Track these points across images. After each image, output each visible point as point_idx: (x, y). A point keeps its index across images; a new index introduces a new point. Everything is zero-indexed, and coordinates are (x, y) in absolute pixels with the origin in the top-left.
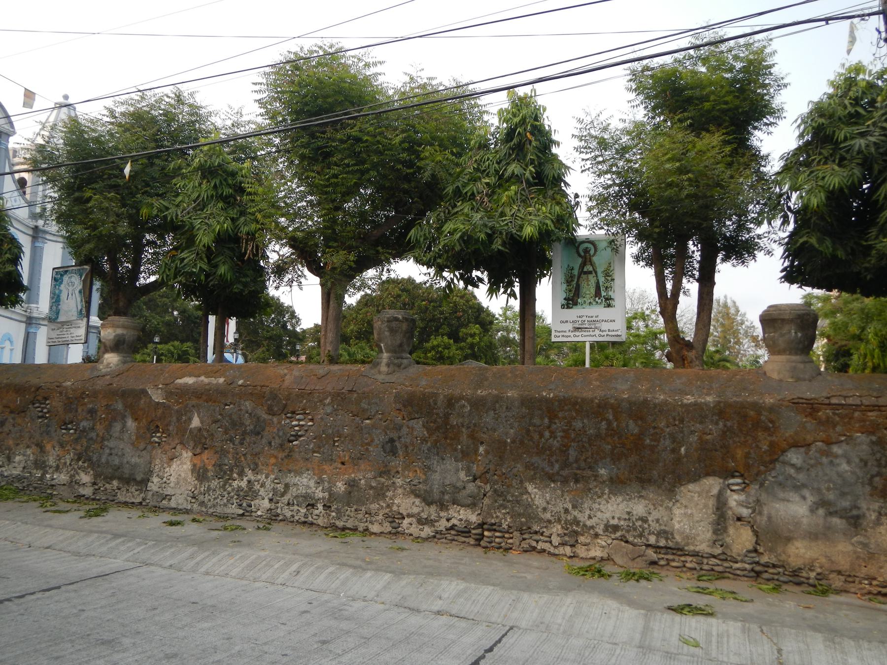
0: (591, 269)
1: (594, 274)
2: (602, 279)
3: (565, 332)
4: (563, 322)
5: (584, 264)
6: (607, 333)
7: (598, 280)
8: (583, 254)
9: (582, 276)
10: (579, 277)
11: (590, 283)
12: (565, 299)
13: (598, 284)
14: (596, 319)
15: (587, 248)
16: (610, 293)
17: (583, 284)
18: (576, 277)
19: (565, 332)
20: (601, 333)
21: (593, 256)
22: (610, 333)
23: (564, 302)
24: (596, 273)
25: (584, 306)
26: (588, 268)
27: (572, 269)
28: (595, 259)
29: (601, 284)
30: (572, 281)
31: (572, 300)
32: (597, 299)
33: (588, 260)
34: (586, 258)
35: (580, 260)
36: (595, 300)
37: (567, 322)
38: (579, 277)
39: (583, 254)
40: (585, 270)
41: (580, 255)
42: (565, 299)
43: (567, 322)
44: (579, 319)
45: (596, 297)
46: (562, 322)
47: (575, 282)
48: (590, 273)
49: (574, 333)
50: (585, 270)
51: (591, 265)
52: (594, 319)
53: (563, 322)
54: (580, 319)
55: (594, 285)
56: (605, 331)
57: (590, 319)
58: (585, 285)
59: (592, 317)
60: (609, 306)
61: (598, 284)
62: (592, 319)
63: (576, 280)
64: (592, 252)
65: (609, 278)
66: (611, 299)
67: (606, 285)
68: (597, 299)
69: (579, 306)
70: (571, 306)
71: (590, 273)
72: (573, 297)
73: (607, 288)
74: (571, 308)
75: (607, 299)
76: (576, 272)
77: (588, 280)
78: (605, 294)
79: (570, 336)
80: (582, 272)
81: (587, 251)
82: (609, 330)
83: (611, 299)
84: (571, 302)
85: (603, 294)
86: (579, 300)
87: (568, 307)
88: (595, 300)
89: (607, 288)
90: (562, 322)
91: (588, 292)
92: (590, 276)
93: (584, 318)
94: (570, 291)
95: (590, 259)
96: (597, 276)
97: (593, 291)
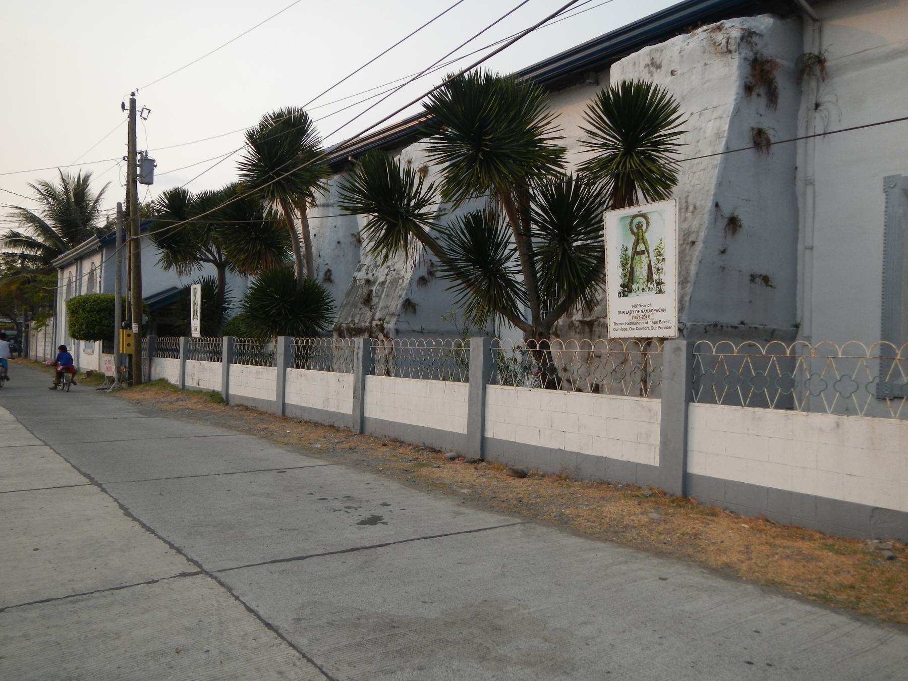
0: (643, 248)
2: (653, 260)
3: (622, 324)
5: (637, 243)
7: (650, 261)
8: (635, 230)
9: (636, 257)
10: (633, 259)
11: (643, 265)
12: (621, 286)
13: (650, 265)
15: (639, 222)
16: (662, 276)
18: (630, 259)
19: (622, 324)
20: (653, 325)
21: (645, 232)
23: (621, 289)
24: (648, 252)
26: (641, 247)
27: (626, 250)
28: (647, 235)
29: (653, 265)
30: (627, 264)
31: (627, 286)
33: (641, 237)
34: (638, 236)
35: (633, 238)
36: (647, 286)
38: (633, 259)
39: (635, 230)
42: (621, 286)
43: (623, 312)
45: (648, 282)
46: (620, 313)
47: (629, 265)
48: (642, 252)
49: (630, 326)
51: (644, 243)
52: (647, 308)
54: (635, 309)
55: (647, 268)
57: (644, 309)
58: (639, 269)
59: (645, 306)
60: (660, 291)
61: (650, 265)
65: (660, 258)
66: (662, 283)
67: (657, 267)
69: (633, 294)
70: (626, 293)
71: (642, 252)
72: (628, 283)
73: (658, 270)
74: (627, 296)
75: (659, 284)
76: (630, 253)
79: (626, 329)
81: (639, 226)
83: (662, 283)
84: (626, 289)
85: (655, 277)
86: (634, 287)
87: (625, 296)
89: (658, 270)
90: (620, 313)
91: (641, 277)
92: (643, 257)
93: (638, 308)
94: (625, 276)
95: (642, 235)
96: (649, 257)
97: (645, 273)
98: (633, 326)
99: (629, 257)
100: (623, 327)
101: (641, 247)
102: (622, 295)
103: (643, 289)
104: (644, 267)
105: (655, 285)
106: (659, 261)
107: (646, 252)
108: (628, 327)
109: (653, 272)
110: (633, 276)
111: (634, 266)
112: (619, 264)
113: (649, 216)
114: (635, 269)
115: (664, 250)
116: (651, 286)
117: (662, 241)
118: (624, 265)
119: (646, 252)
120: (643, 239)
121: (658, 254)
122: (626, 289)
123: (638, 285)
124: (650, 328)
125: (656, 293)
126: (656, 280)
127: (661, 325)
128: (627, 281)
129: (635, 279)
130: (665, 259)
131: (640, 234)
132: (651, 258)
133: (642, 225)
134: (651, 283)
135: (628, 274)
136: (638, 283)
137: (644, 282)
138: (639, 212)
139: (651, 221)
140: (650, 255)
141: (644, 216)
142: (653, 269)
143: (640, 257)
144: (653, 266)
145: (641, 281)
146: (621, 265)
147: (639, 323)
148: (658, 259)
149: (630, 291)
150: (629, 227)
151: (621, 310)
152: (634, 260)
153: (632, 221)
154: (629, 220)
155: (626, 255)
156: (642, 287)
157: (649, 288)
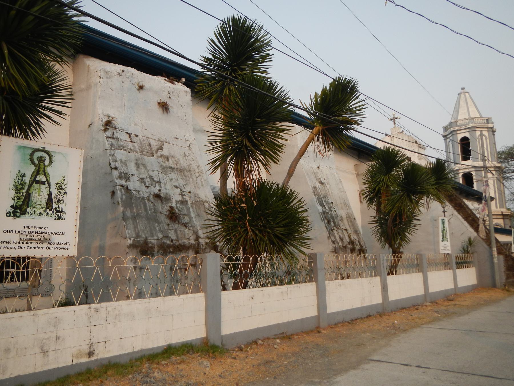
0: (44, 179)
1: (47, 185)
2: (54, 192)
3: (8, 243)
4: (7, 231)
5: (37, 173)
6: (56, 245)
7: (50, 192)
8: (37, 162)
9: (34, 184)
10: (30, 186)
11: (41, 193)
12: (12, 207)
14: (45, 231)
15: (42, 157)
16: (62, 206)
17: (35, 195)
19: (8, 243)
20: (49, 245)
21: (47, 166)
22: (58, 246)
23: (10, 210)
24: (49, 184)
25: (33, 216)
26: (41, 177)
27: (24, 176)
28: (49, 170)
29: (53, 196)
30: (22, 188)
31: (20, 209)
32: (48, 210)
33: (42, 169)
34: (39, 168)
35: (33, 168)
36: (45, 211)
37: (11, 231)
38: (30, 186)
39: (37, 162)
40: (38, 179)
41: (33, 163)
42: (12, 207)
43: (11, 231)
44: (26, 229)
45: (47, 208)
46: (6, 231)
47: (25, 190)
50: (38, 179)
51: (45, 175)
52: (43, 230)
53: (7, 231)
54: (28, 230)
56: (54, 244)
57: (39, 230)
58: (37, 195)
59: (41, 228)
60: (60, 218)
62: (41, 231)
63: (26, 188)
64: (47, 162)
65: (62, 192)
66: (62, 211)
67: (58, 198)
68: (48, 210)
69: (27, 216)
71: (43, 183)
72: (21, 205)
73: (59, 200)
76: (27, 180)
77: (40, 190)
78: (57, 206)
79: (13, 248)
80: (34, 181)
81: (41, 160)
82: (58, 243)
83: (62, 211)
85: (55, 206)
86: (28, 210)
87: (15, 216)
88: (45, 211)
89: (59, 200)
90: (6, 231)
92: (43, 187)
93: (32, 229)
94: (19, 199)
95: (44, 168)
96: (50, 187)
97: (44, 201)
98: (22, 245)
99: (25, 183)
100: (11, 245)
101: (41, 177)
102: (12, 215)
103: (40, 213)
104: (43, 195)
105: (55, 212)
106: (61, 193)
107: (46, 183)
108: (14, 245)
109: (53, 201)
110: (29, 201)
111: (31, 192)
112: (12, 186)
113: (52, 154)
114: (33, 195)
115: (66, 186)
116: (50, 213)
117: (65, 178)
118: (18, 189)
119: (46, 183)
120: (44, 171)
121: (60, 187)
122: (18, 211)
123: (34, 209)
124: (45, 248)
125: (55, 219)
126: (55, 208)
127: (58, 246)
128: (21, 203)
129: (32, 203)
130: (66, 193)
131: (42, 167)
132: (52, 190)
133: (45, 160)
134: (50, 210)
135: (23, 198)
136: (34, 207)
137: (42, 208)
138: (42, 147)
139: (55, 158)
140: (51, 187)
141: (48, 153)
142: (53, 199)
143: (40, 186)
144: (53, 197)
145: (38, 206)
146: (14, 188)
147: (32, 243)
148: (59, 192)
149: (24, 213)
150: (29, 157)
151: (9, 229)
152: (32, 188)
153: (32, 154)
154: (30, 151)
155: (22, 180)
156: (39, 211)
157: (48, 214)
